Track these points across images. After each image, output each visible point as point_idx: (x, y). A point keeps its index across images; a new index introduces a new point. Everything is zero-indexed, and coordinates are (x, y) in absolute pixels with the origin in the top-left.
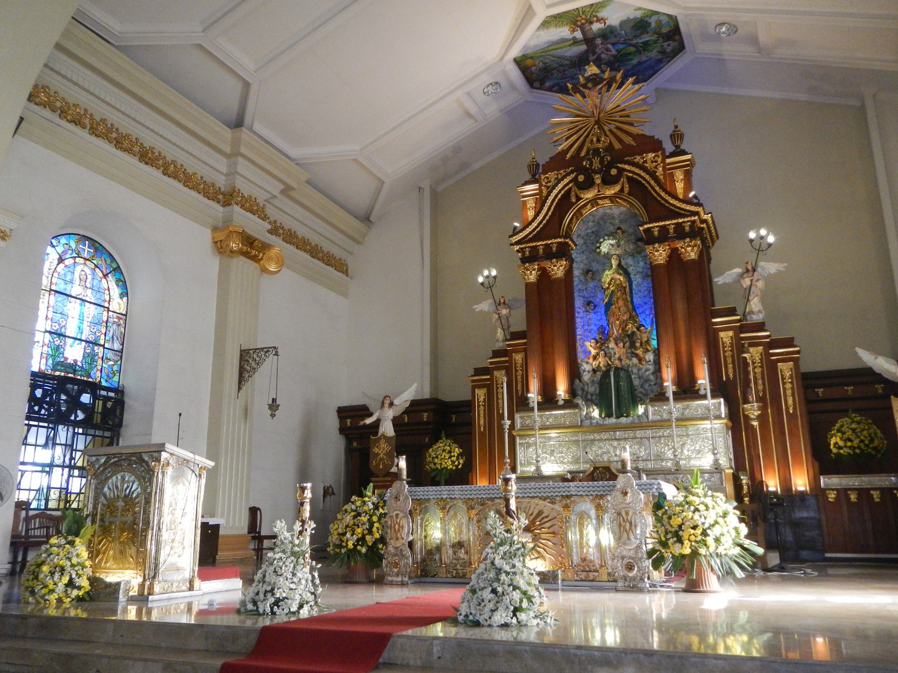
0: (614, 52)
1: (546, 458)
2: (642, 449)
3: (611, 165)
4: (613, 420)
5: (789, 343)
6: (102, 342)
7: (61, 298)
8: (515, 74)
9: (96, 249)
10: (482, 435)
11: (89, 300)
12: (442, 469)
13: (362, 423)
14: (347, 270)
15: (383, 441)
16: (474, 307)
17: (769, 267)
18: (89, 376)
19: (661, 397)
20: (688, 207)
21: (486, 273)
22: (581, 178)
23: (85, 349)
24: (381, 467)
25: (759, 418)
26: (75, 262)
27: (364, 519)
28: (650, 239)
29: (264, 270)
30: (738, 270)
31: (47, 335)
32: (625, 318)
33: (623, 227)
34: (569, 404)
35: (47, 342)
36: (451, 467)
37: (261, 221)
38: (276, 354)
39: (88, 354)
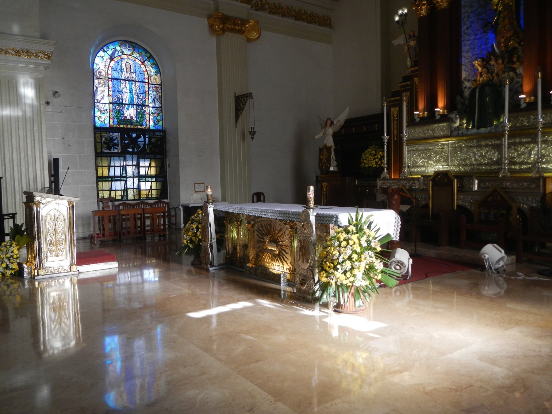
1: (425, 162)
2: (496, 155)
6: (147, 104)
7: (116, 82)
9: (134, 48)
11: (134, 80)
12: (369, 167)
14: (330, 23)
16: (393, 42)
18: (142, 125)
21: (400, 12)
23: (137, 109)
24: (324, 168)
26: (121, 59)
27: (194, 226)
29: (249, 40)
31: (111, 105)
32: (508, 35)
34: (444, 118)
35: (111, 109)
36: (375, 166)
37: (246, 5)
38: (252, 98)
39: (139, 112)
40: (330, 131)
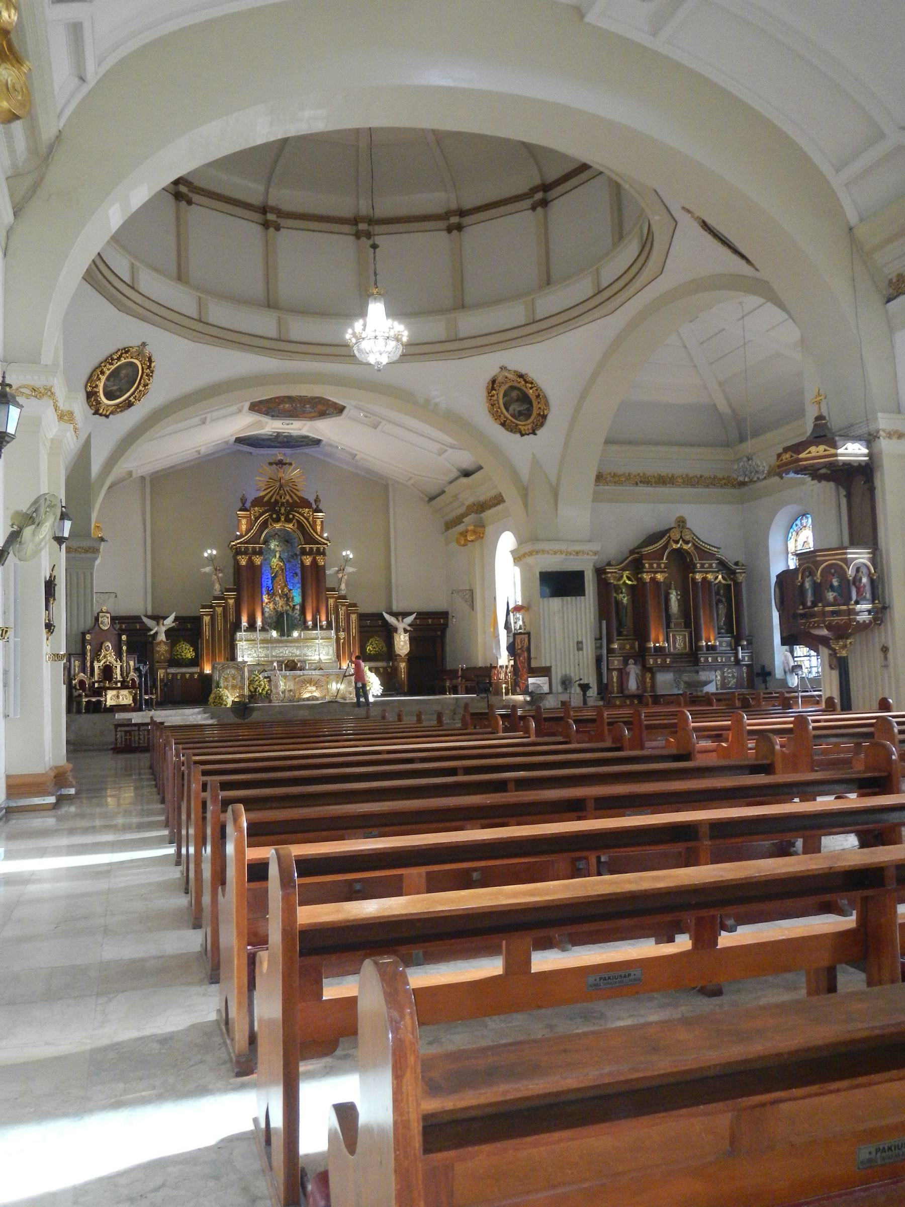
0: (285, 439)
3: (288, 513)
4: (285, 638)
5: (354, 605)
8: (233, 439)
10: (207, 641)
13: (149, 634)
15: (162, 644)
17: (350, 569)
19: (306, 628)
20: (323, 541)
22: (274, 516)
25: (344, 638)
28: (304, 552)
30: (337, 569)
33: (279, 533)
34: (263, 629)
38: (116, 597)
40: (164, 629)
